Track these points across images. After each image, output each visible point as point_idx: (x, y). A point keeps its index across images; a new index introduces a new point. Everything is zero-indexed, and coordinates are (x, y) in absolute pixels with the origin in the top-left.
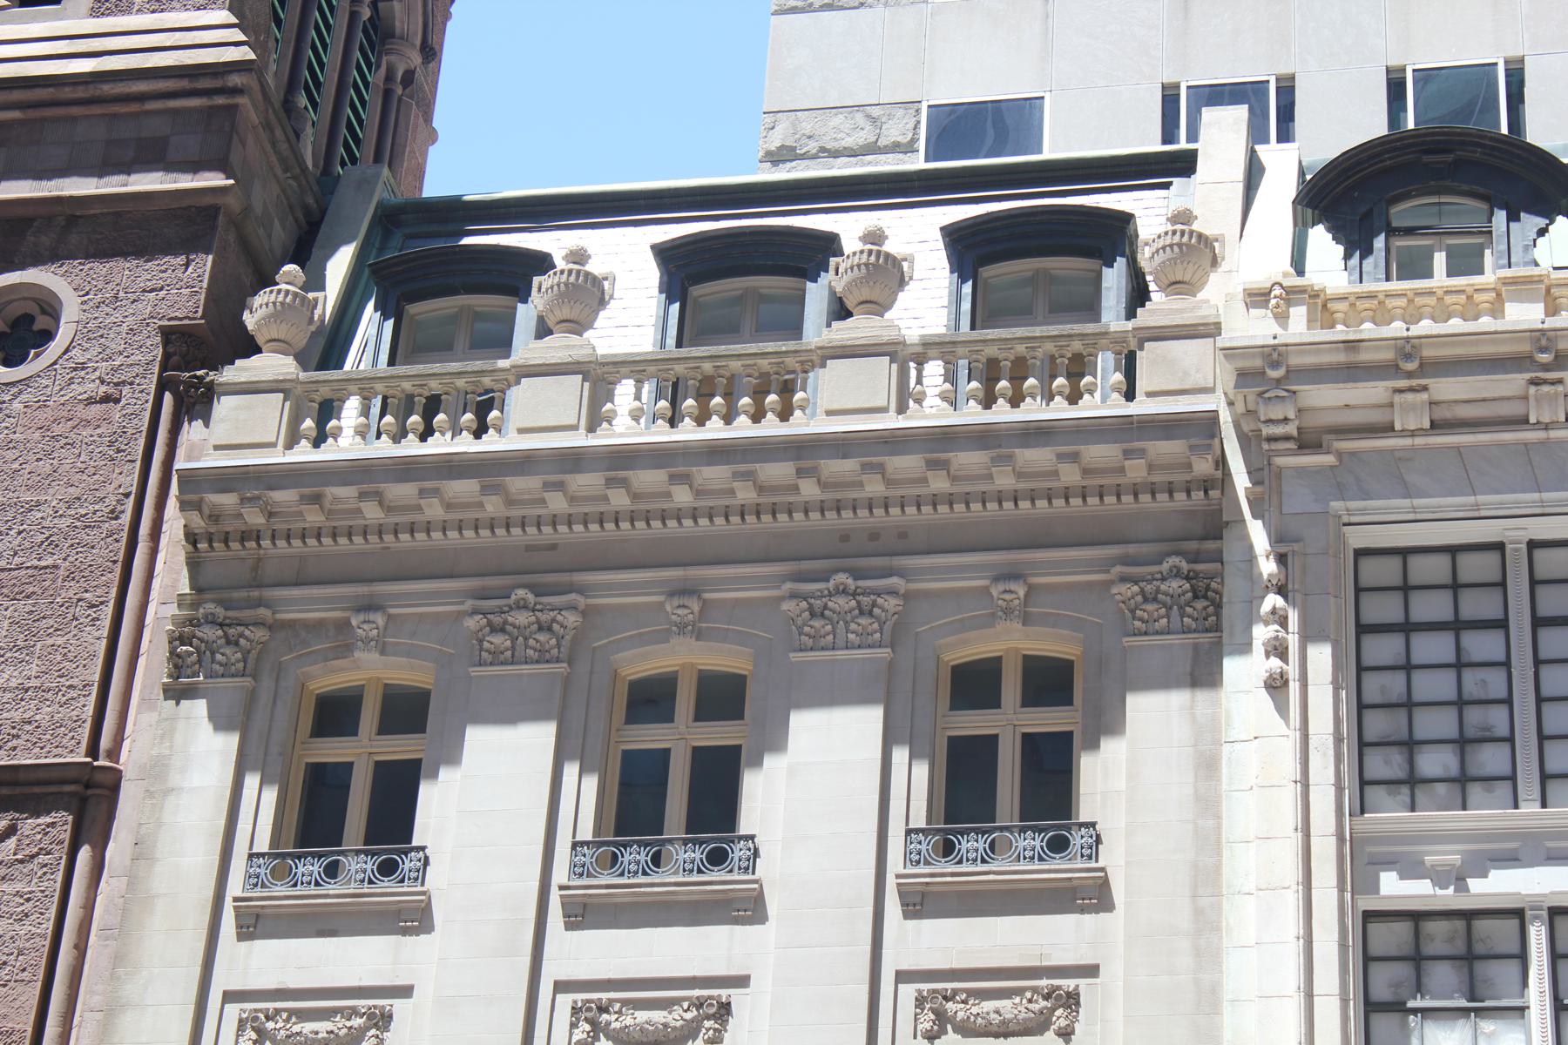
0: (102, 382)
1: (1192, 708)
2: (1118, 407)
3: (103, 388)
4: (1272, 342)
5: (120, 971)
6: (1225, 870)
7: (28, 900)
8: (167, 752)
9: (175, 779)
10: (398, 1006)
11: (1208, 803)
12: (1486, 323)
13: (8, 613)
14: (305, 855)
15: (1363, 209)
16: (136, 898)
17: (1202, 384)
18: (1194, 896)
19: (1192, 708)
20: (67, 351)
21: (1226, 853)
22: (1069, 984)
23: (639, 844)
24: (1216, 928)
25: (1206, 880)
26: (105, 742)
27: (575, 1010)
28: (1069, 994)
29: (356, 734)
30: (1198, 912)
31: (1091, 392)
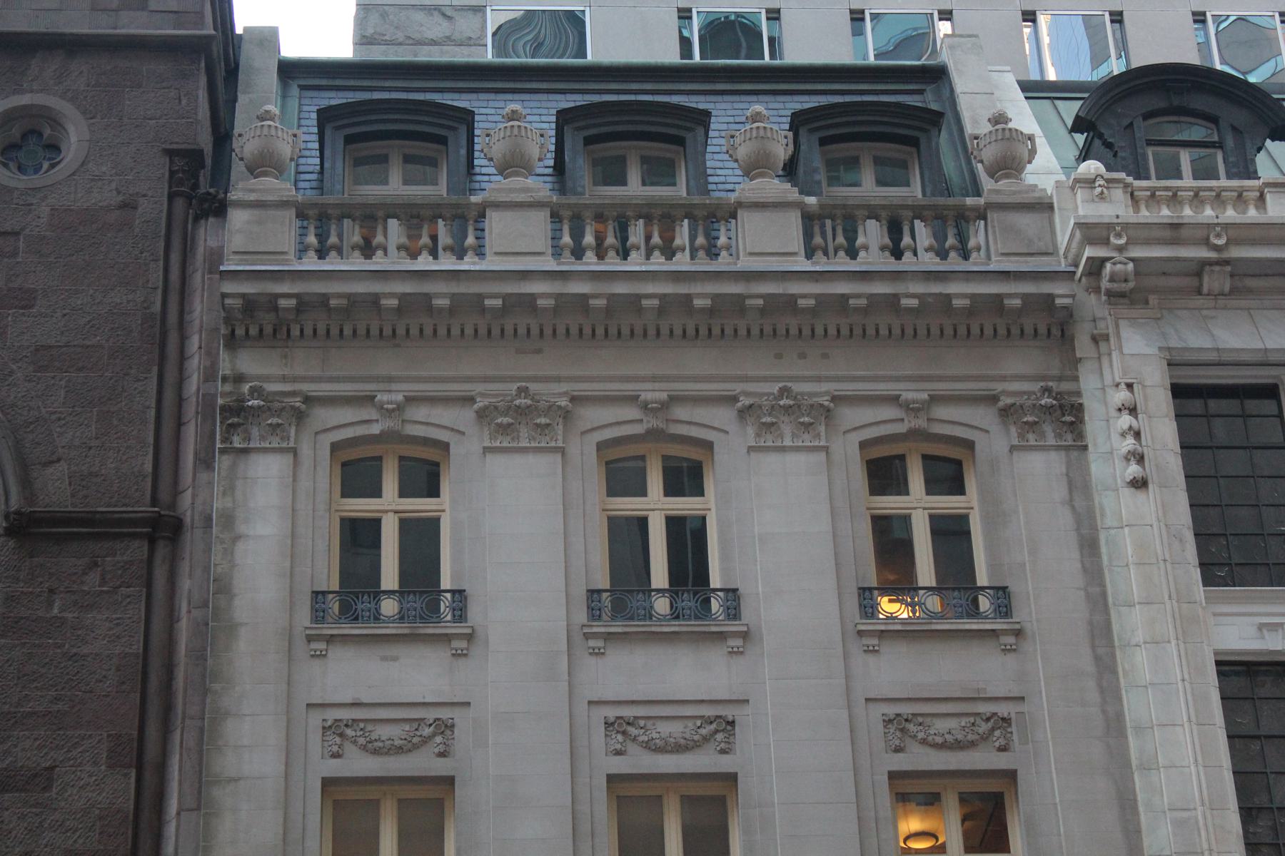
0: (119, 193)
1: (1071, 500)
2: (888, 263)
3: (121, 198)
4: (1116, 221)
5: (216, 686)
6: (1115, 628)
7: (118, 625)
8: (230, 505)
9: (242, 528)
10: (456, 714)
11: (1093, 572)
12: (1252, 214)
13: (63, 383)
14: (409, 593)
15: (1126, 122)
16: (216, 626)
17: (1044, 249)
18: (1093, 647)
19: (1071, 500)
20: (83, 164)
21: (1113, 613)
22: (1003, 709)
23: (414, 593)
24: (1114, 672)
25: (1101, 633)
26: (164, 496)
27: (608, 724)
28: (1003, 719)
29: (928, 494)
30: (1097, 659)
31: (866, 248)
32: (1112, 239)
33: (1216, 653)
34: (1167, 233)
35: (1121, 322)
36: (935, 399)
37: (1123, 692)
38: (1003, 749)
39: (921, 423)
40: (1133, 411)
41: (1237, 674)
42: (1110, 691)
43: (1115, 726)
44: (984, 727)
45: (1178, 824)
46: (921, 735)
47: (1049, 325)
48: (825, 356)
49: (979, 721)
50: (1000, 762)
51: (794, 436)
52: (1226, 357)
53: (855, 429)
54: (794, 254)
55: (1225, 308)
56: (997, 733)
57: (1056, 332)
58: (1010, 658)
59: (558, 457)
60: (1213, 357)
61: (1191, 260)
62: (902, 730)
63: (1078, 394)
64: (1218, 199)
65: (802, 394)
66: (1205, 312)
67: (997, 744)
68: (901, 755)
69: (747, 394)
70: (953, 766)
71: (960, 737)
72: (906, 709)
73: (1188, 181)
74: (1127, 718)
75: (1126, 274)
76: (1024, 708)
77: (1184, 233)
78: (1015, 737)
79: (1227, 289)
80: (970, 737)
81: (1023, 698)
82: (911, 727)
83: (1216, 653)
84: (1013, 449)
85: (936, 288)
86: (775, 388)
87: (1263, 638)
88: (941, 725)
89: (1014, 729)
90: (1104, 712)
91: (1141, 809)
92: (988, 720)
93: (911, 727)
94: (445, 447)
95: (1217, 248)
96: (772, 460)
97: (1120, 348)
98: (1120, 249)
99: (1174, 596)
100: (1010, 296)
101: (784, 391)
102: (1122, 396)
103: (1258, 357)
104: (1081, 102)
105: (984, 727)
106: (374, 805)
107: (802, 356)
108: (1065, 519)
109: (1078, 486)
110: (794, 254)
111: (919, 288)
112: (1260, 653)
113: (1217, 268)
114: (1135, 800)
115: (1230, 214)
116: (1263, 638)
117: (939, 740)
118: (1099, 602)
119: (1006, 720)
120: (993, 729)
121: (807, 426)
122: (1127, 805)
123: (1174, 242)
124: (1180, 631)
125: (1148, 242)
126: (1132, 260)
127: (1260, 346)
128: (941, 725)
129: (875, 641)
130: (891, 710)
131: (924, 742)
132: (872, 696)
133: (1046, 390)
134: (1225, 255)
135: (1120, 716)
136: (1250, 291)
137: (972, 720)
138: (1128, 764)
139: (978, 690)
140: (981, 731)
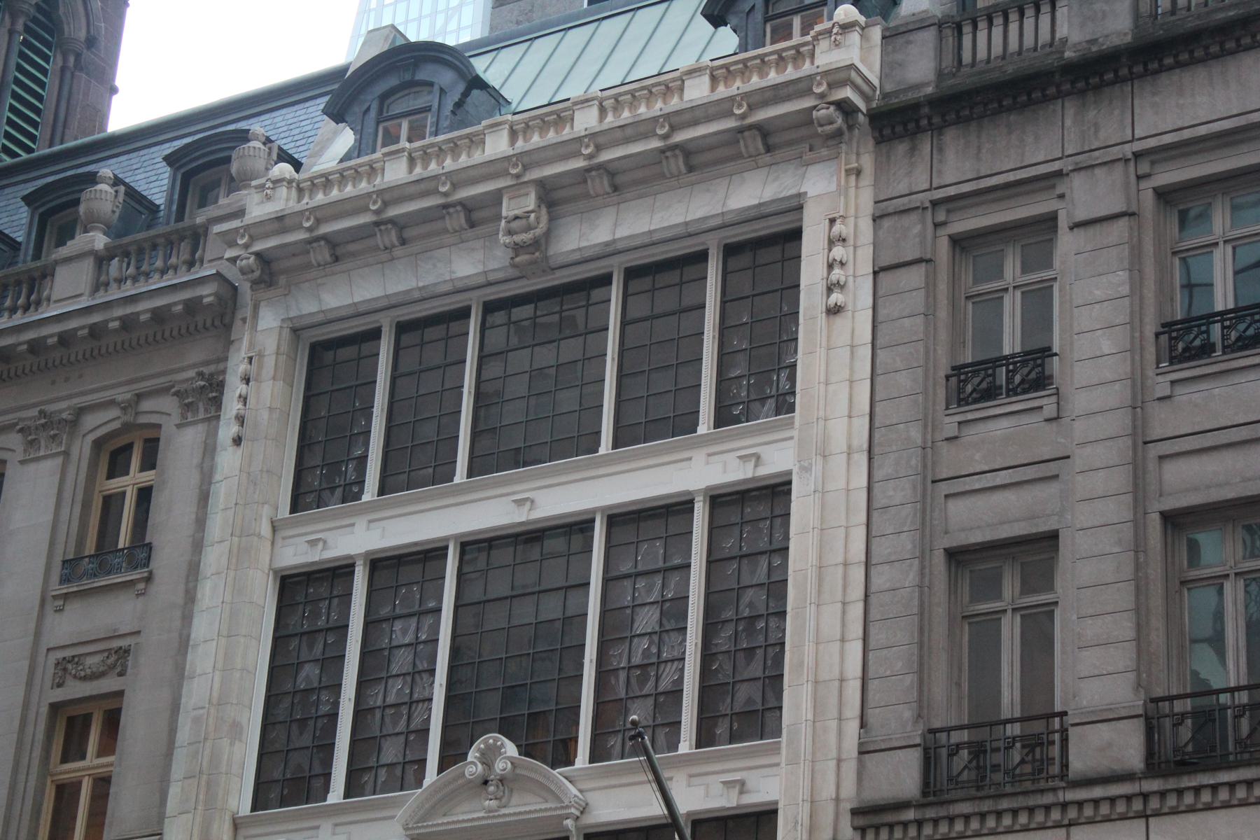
11: (201, 523)
25: (193, 572)
32: (240, 242)
34: (276, 225)
35: (262, 304)
36: (139, 397)
38: (121, 674)
39: (129, 418)
40: (247, 380)
42: (187, 618)
43: (184, 644)
47: (218, 318)
48: (81, 376)
51: (206, 410)
52: (331, 316)
53: (92, 431)
54: (81, 295)
55: (334, 274)
57: (217, 323)
58: (141, 598)
60: (320, 318)
61: (296, 243)
63: (224, 372)
64: (440, 152)
65: (55, 412)
66: (319, 281)
69: (21, 419)
70: (87, 694)
72: (68, 653)
73: (404, 143)
75: (249, 266)
77: (287, 222)
79: (328, 258)
80: (101, 669)
81: (139, 632)
82: (70, 666)
84: (179, 426)
85: (129, 310)
86: (34, 412)
93: (70, 666)
94: (159, 426)
95: (446, 194)
96: (32, 467)
97: (254, 327)
98: (246, 246)
99: (238, 532)
100: (175, 304)
101: (42, 413)
102: (243, 367)
103: (351, 311)
104: (327, 98)
106: (87, 719)
107: (67, 380)
108: (195, 478)
109: (210, 449)
110: (81, 295)
111: (119, 312)
113: (315, 245)
115: (449, 164)
118: (198, 546)
121: (54, 437)
122: (175, 708)
123: (284, 231)
124: (234, 561)
125: (266, 236)
126: (258, 255)
127: (349, 301)
128: (90, 661)
129: (61, 603)
130: (60, 655)
132: (51, 646)
133: (201, 374)
134: (316, 233)
135: (189, 636)
136: (353, 255)
138: (183, 675)
139: (115, 631)
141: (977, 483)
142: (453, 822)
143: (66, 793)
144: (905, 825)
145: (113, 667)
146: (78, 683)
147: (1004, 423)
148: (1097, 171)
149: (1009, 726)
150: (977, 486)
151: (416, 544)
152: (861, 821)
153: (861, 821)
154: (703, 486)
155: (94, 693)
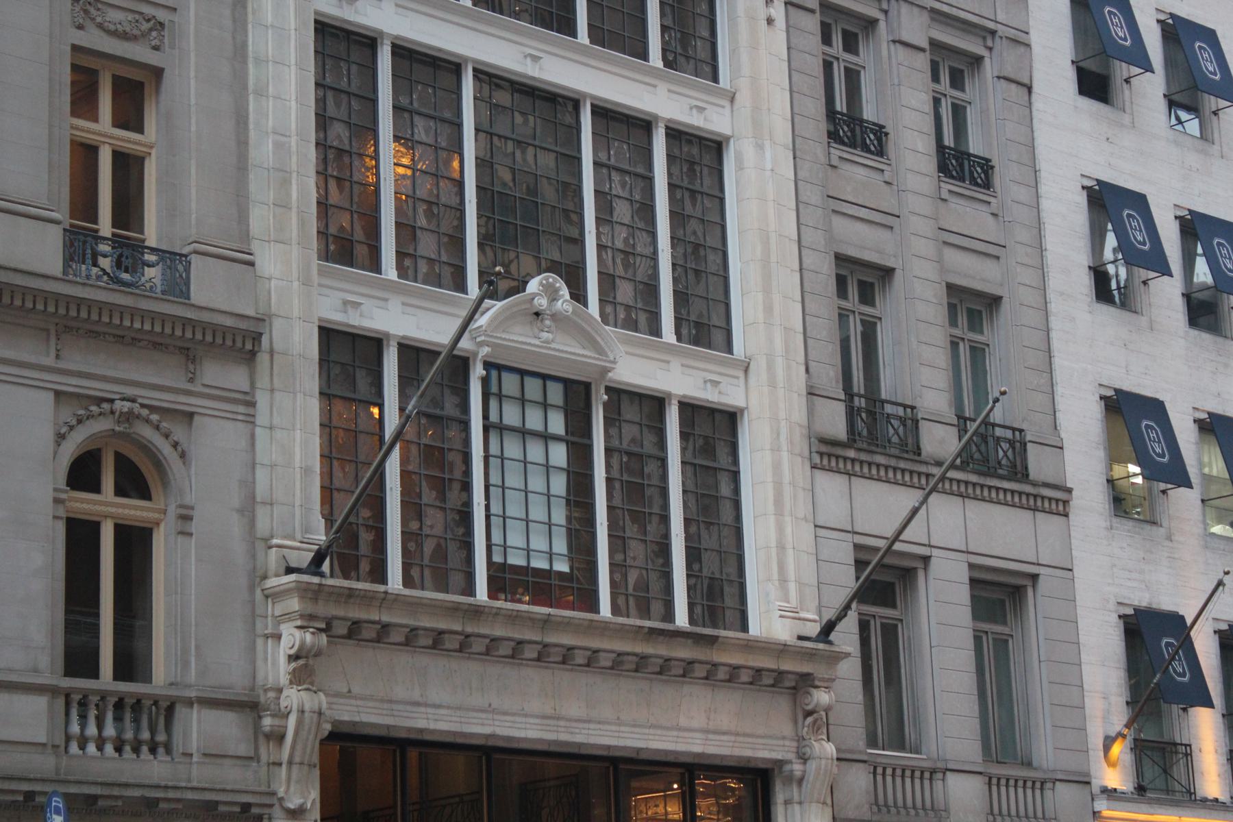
22: (161, 15)
33: (316, 13)
37: (250, 26)
38: (156, 48)
41: (360, 43)
43: (240, 53)
44: (145, 26)
45: (278, 146)
46: (99, 20)
49: (141, 20)
50: (152, 58)
56: (154, 34)
59: (1026, 90)
62: (86, 12)
67: (153, 43)
68: (81, 32)
70: (119, 53)
71: (128, 29)
74: (250, 48)
76: (176, 18)
78: (166, 40)
81: (175, 9)
83: (316, 13)
87: (341, 7)
88: (114, 16)
89: (166, 33)
90: (234, 38)
91: (251, 126)
92: (149, 20)
93: (92, 10)
105: (145, 26)
112: (337, 19)
114: (247, 117)
116: (341, 7)
117: (112, 27)
119: (162, 25)
120: (151, 30)
122: (241, 120)
131: (100, 26)
135: (244, 45)
137: (137, 17)
138: (245, 87)
140: (143, 28)
141: (863, 213)
142: (509, 340)
143: (85, 154)
144: (845, 459)
145: (144, 35)
146: (102, 34)
147: (861, 170)
148: (916, 10)
149: (997, 429)
150: (850, 212)
151: (440, 50)
152: (824, 449)
153: (824, 449)
154: (395, 33)
155: (128, 56)
